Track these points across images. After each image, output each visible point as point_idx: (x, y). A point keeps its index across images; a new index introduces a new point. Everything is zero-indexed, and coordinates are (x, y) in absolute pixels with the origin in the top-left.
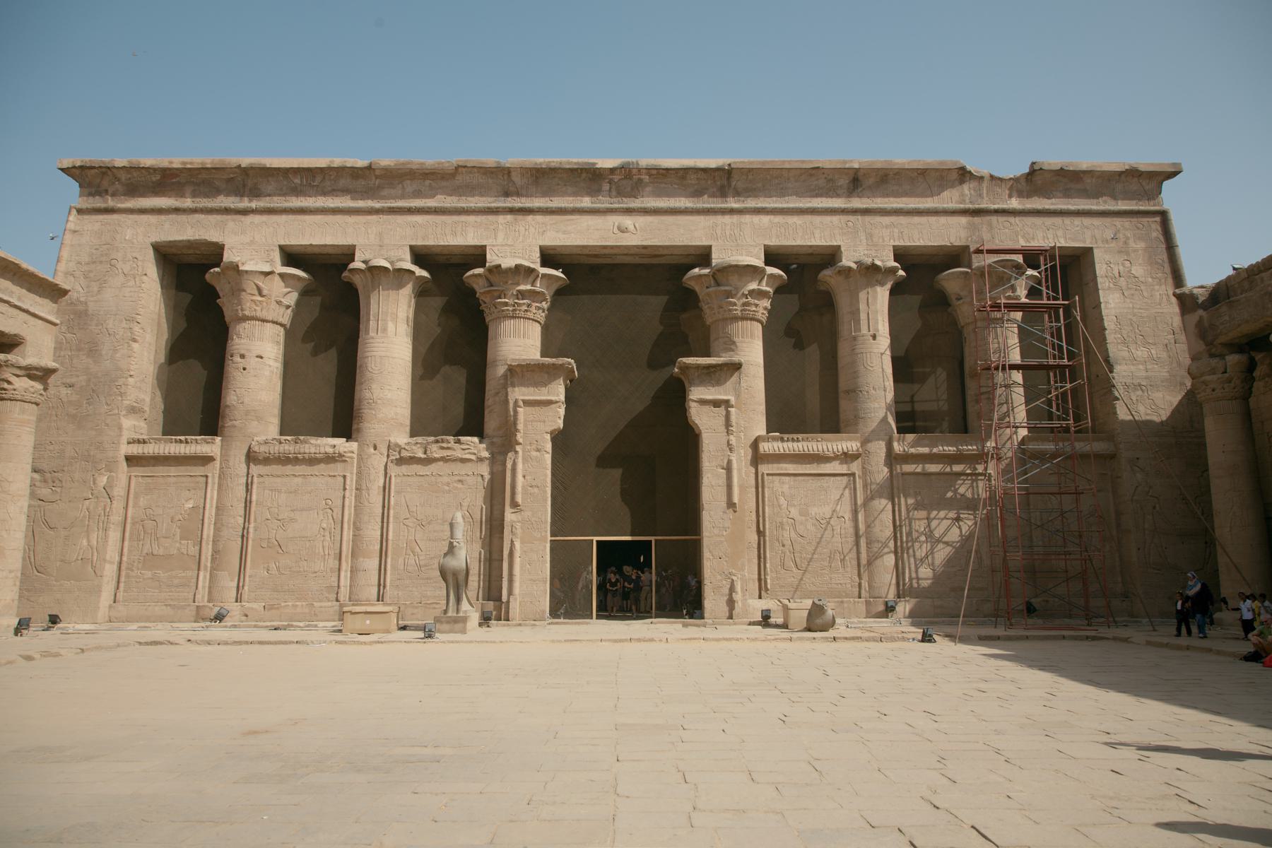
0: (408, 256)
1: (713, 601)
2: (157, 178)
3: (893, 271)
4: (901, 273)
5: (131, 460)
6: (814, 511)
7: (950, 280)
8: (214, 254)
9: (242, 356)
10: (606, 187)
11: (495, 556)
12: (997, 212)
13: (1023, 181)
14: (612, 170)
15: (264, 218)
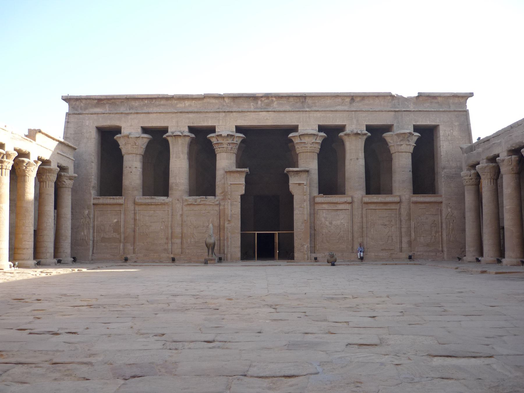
0: (187, 129)
1: (297, 255)
2: (96, 101)
3: (365, 134)
4: (369, 134)
5: (94, 204)
6: (334, 223)
7: (387, 136)
8: (118, 130)
9: (130, 167)
10: (259, 102)
11: (221, 238)
12: (405, 111)
13: (415, 99)
14: (262, 97)
15: (135, 115)
